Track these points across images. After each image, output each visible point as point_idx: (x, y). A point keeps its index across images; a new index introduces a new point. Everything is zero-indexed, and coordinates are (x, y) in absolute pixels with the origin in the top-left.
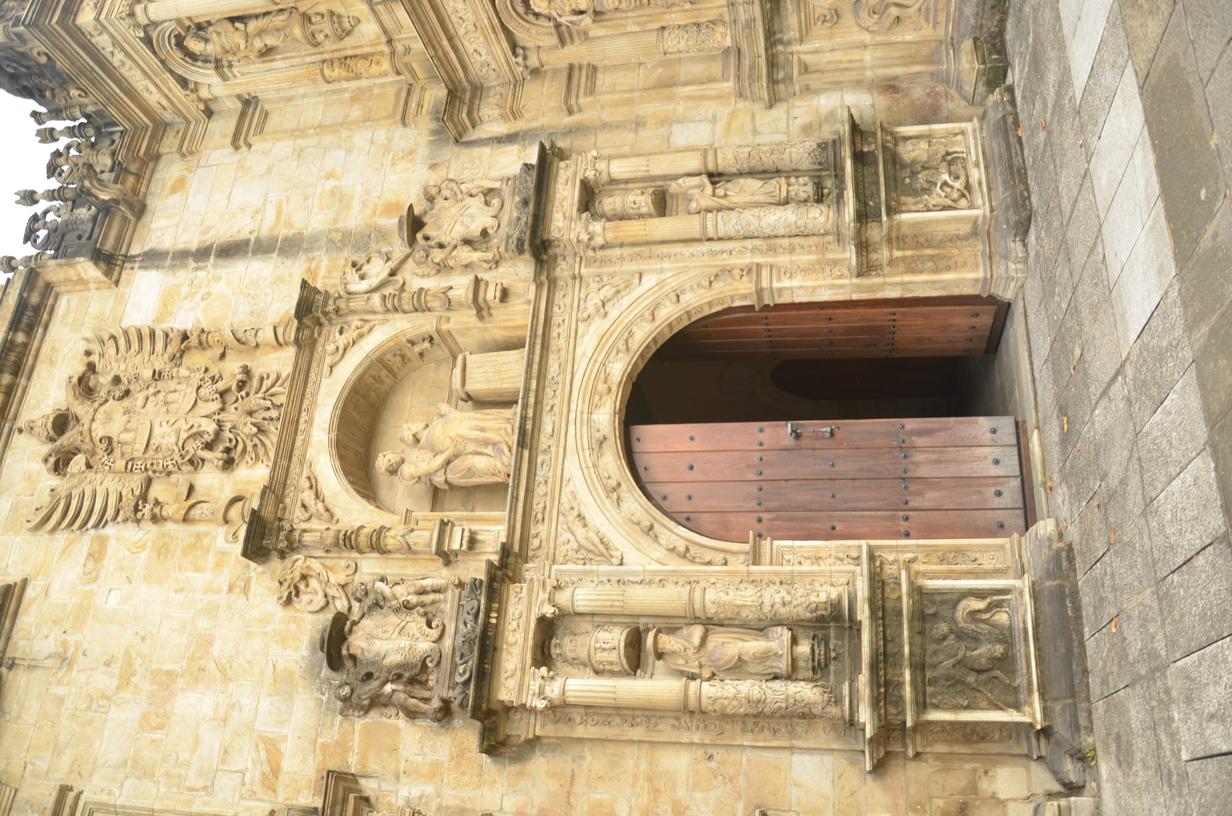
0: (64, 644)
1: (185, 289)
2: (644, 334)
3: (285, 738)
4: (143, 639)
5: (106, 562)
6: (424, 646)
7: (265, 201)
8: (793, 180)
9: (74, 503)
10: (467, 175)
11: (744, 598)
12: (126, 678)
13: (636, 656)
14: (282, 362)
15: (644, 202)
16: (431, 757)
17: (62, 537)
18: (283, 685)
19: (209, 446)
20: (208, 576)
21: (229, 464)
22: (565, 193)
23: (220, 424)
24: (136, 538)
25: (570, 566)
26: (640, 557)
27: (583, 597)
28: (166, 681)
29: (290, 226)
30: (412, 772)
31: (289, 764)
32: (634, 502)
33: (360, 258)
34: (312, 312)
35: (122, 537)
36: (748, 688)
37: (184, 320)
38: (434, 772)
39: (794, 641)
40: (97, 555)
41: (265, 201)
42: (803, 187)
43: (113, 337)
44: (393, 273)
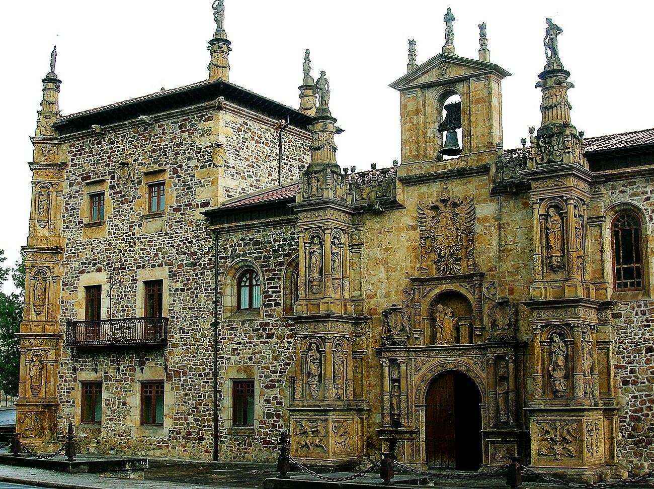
0: (392, 228)
1: (488, 224)
2: (471, 374)
3: (377, 298)
4: (395, 251)
5: (411, 232)
6: (394, 331)
7: (517, 243)
8: (506, 415)
9: (423, 216)
10: (521, 314)
11: (403, 405)
12: (386, 250)
13: (394, 381)
14: (462, 269)
15: (501, 374)
16: (376, 335)
17: (416, 214)
18: (388, 295)
19: (439, 255)
20: (409, 265)
21: (435, 263)
22: (501, 351)
23: (445, 256)
24: (417, 239)
25: (413, 363)
26: (415, 379)
27: (403, 368)
28: (386, 261)
29: (508, 256)
30: (373, 331)
31: (372, 301)
32: (430, 376)
33: (496, 285)
34: (474, 277)
35: (416, 234)
36: (387, 405)
37: (478, 229)
38: (373, 337)
39: (397, 415)
40: (414, 228)
41: (517, 243)
42: (503, 418)
43: (472, 205)
44: (489, 298)
